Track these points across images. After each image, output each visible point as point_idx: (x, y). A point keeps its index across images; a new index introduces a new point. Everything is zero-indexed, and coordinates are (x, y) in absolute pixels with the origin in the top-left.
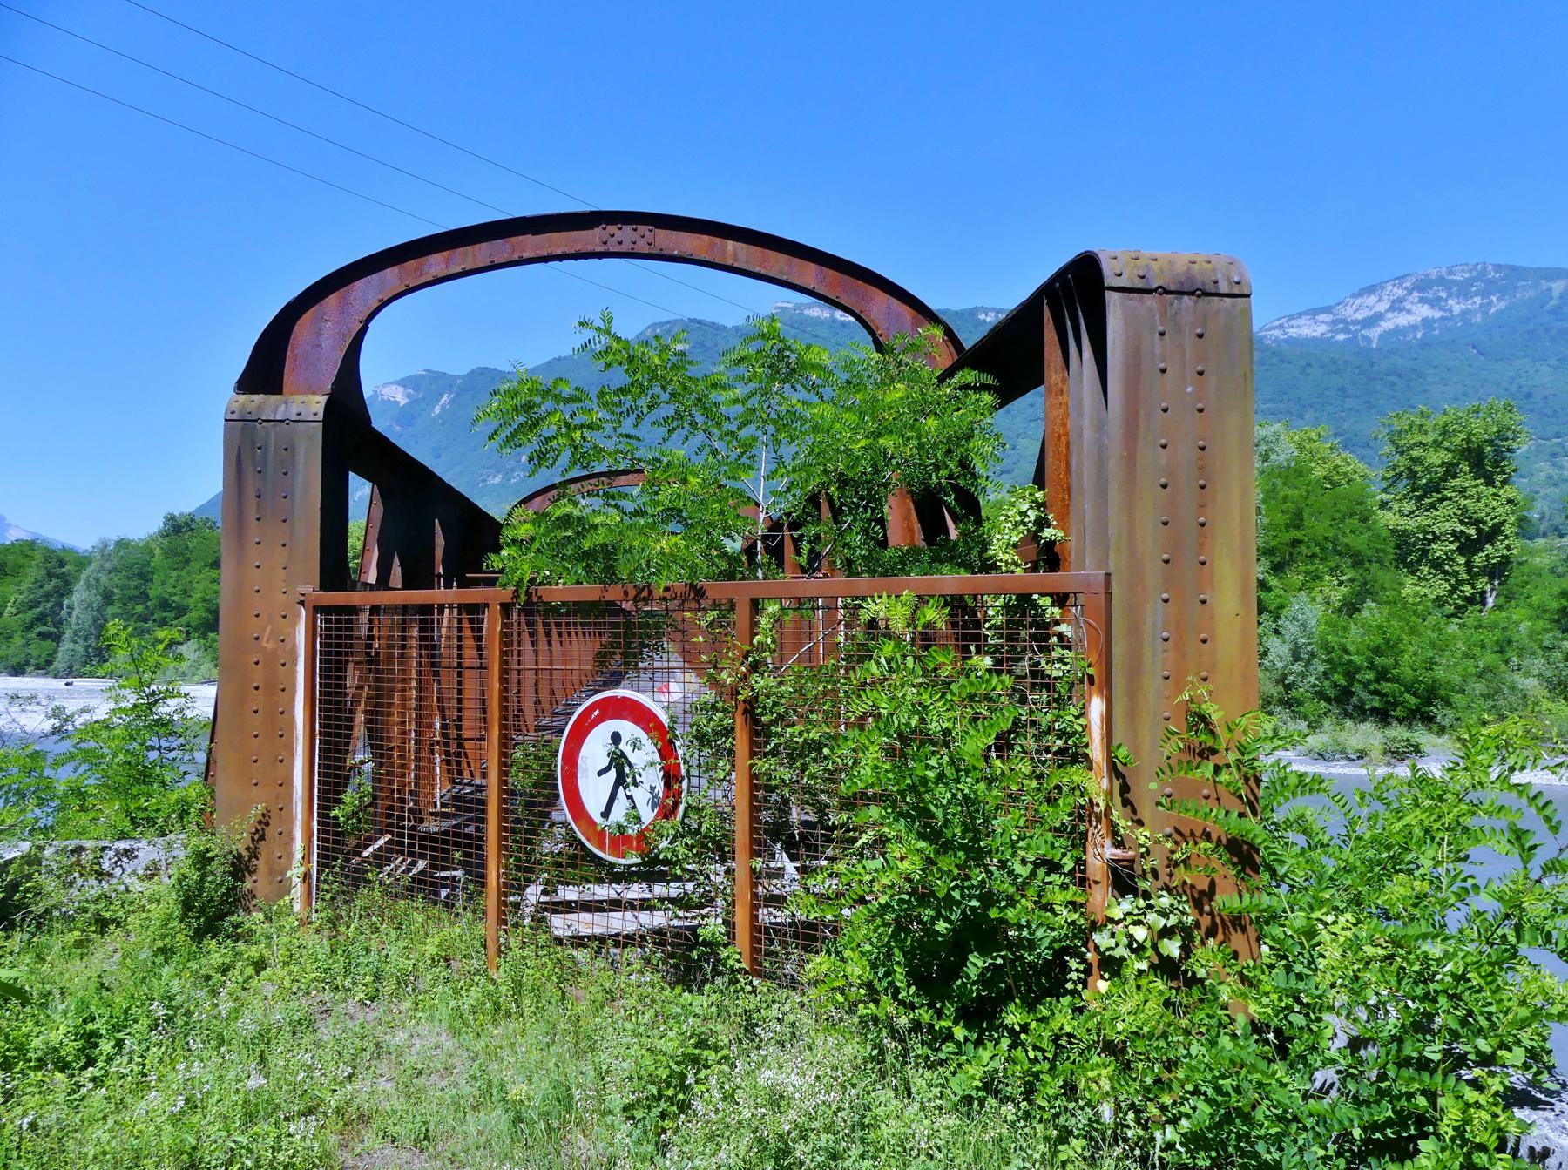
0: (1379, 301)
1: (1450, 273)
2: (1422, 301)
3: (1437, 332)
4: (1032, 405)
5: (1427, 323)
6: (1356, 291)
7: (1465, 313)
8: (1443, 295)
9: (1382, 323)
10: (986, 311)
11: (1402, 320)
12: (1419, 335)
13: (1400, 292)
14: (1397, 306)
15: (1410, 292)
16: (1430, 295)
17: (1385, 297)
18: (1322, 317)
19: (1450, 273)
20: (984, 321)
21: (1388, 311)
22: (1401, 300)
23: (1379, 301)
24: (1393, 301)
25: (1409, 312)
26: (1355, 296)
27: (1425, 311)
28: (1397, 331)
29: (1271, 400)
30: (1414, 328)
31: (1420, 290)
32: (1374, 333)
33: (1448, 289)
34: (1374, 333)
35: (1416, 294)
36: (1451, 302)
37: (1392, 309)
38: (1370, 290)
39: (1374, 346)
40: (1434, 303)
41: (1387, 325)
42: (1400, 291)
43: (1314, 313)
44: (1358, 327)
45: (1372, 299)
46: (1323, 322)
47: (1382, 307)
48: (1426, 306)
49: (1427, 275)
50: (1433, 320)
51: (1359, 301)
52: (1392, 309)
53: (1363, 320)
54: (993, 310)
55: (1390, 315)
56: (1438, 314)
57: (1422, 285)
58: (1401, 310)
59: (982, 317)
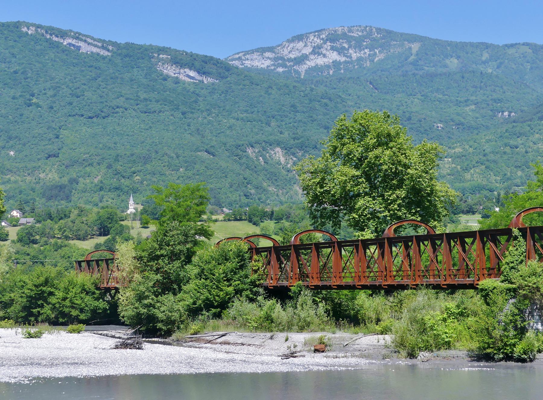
0: (305, 46)
1: (350, 31)
2: (333, 49)
3: (342, 71)
4: (71, 104)
5: (336, 64)
6: (290, 37)
7: (359, 59)
8: (346, 46)
9: (307, 62)
10: (28, 26)
11: (320, 61)
12: (331, 72)
13: (318, 41)
14: (317, 51)
15: (325, 43)
16: (337, 44)
17: (309, 44)
18: (267, 54)
19: (350, 31)
20: (27, 33)
21: (311, 53)
22: (319, 47)
23: (305, 46)
24: (314, 47)
25: (324, 56)
26: (289, 41)
27: (334, 56)
28: (317, 68)
29: (246, 111)
30: (328, 67)
31: (332, 40)
32: (303, 68)
33: (349, 42)
34: (303, 68)
35: (329, 44)
36: (351, 51)
37: (313, 52)
38: (299, 38)
39: (302, 77)
40: (341, 51)
41: (310, 64)
42: (318, 41)
43: (262, 51)
44: (292, 64)
45: (301, 44)
46: (268, 58)
47: (307, 51)
48: (335, 53)
49: (335, 31)
50: (340, 63)
51: (292, 45)
52: (313, 52)
53: (295, 59)
54: (33, 25)
55: (312, 57)
56: (343, 59)
57: (333, 38)
58: (319, 54)
59: (25, 29)
